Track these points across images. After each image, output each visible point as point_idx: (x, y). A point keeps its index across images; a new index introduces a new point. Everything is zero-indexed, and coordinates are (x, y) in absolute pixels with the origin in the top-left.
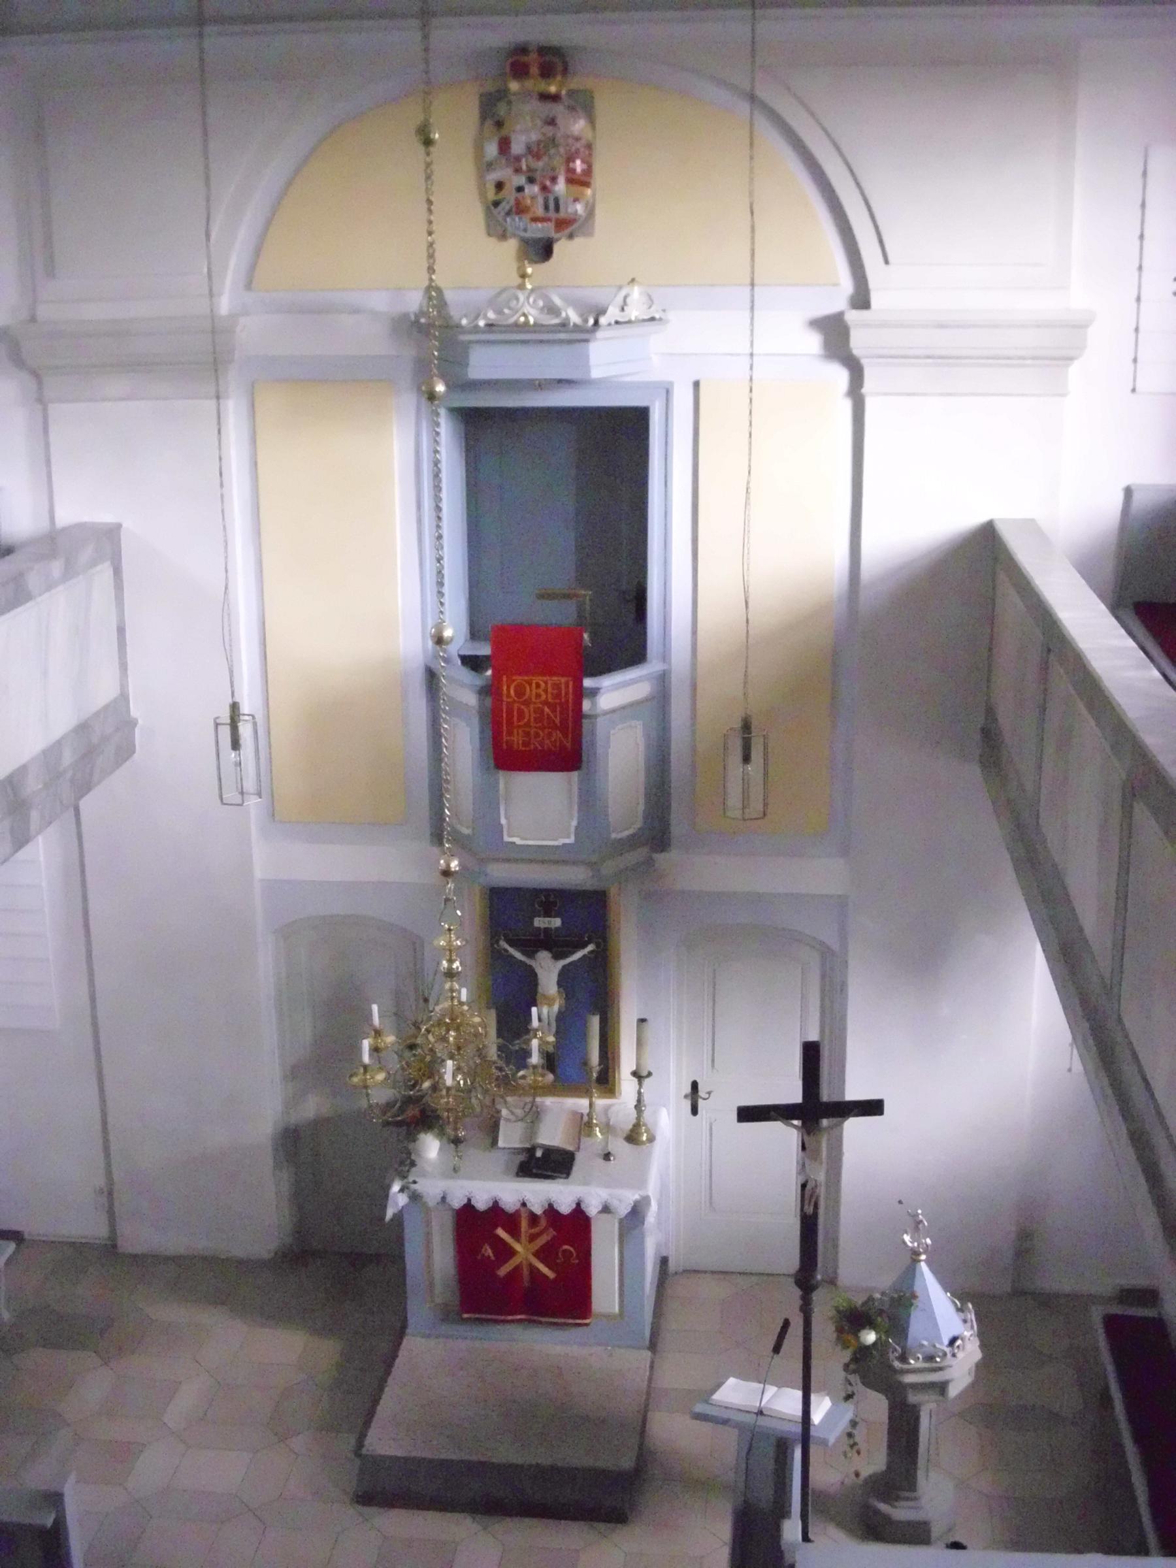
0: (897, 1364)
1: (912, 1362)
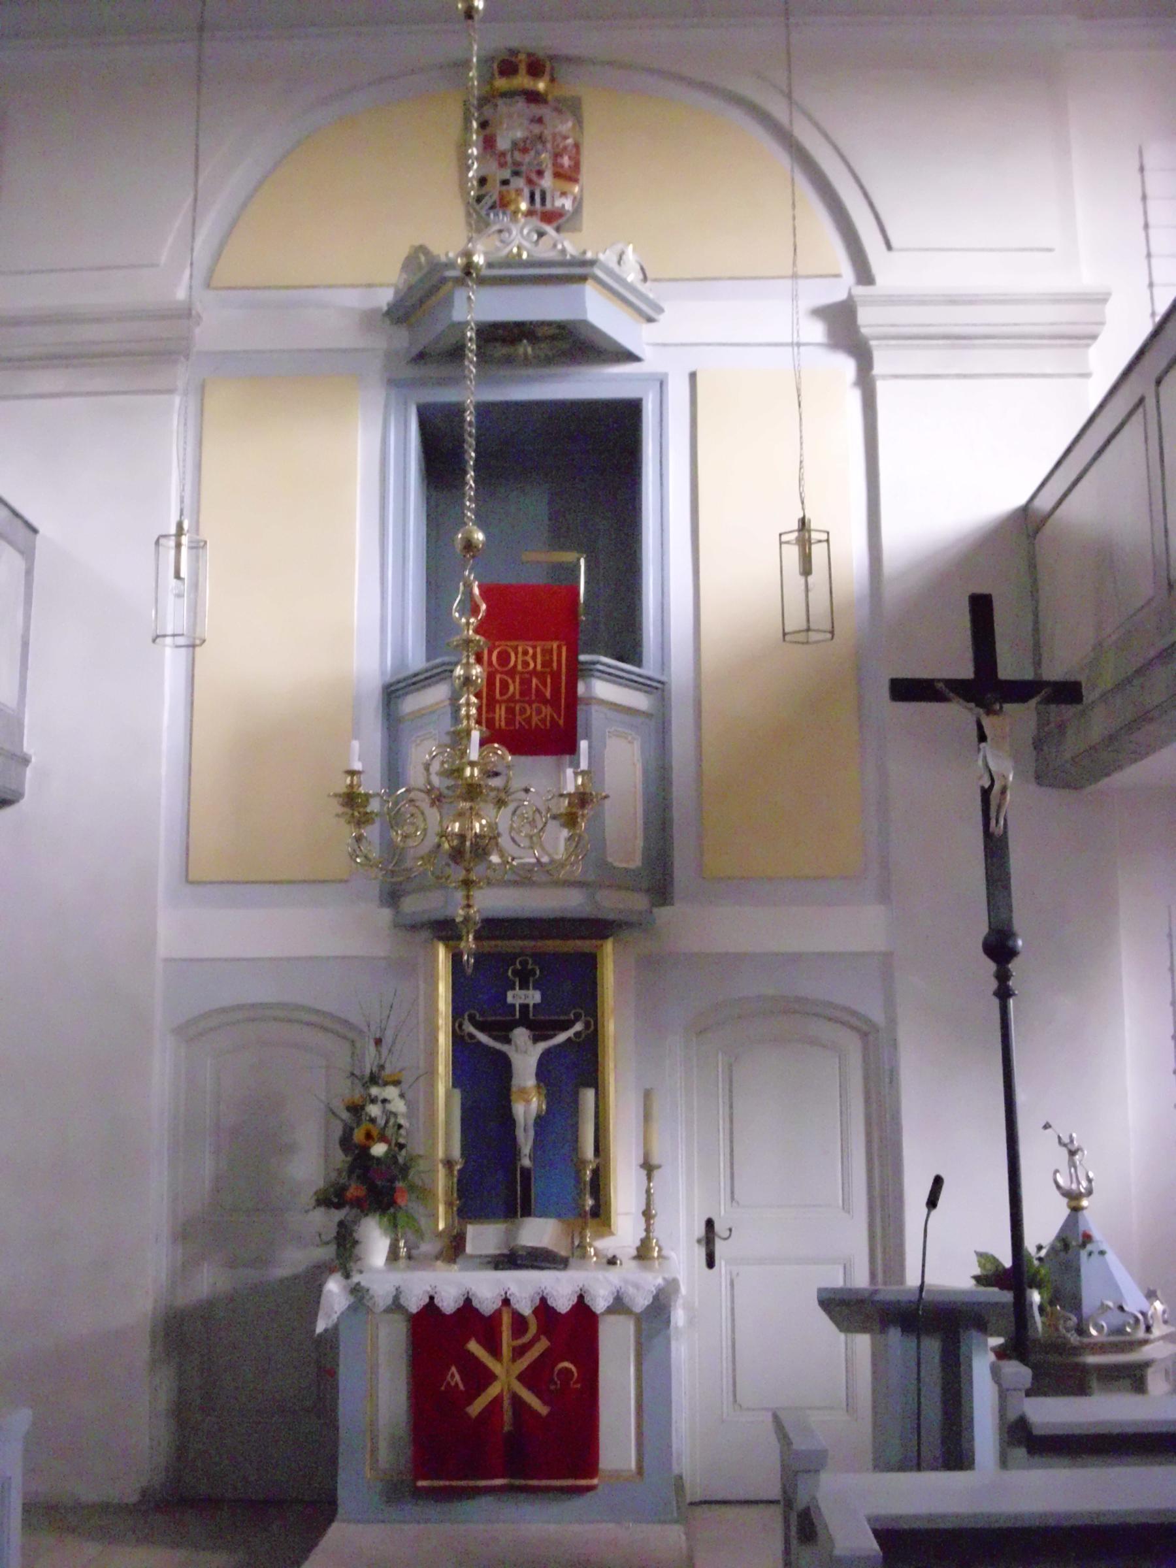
0: (1074, 1338)
1: (1093, 1332)
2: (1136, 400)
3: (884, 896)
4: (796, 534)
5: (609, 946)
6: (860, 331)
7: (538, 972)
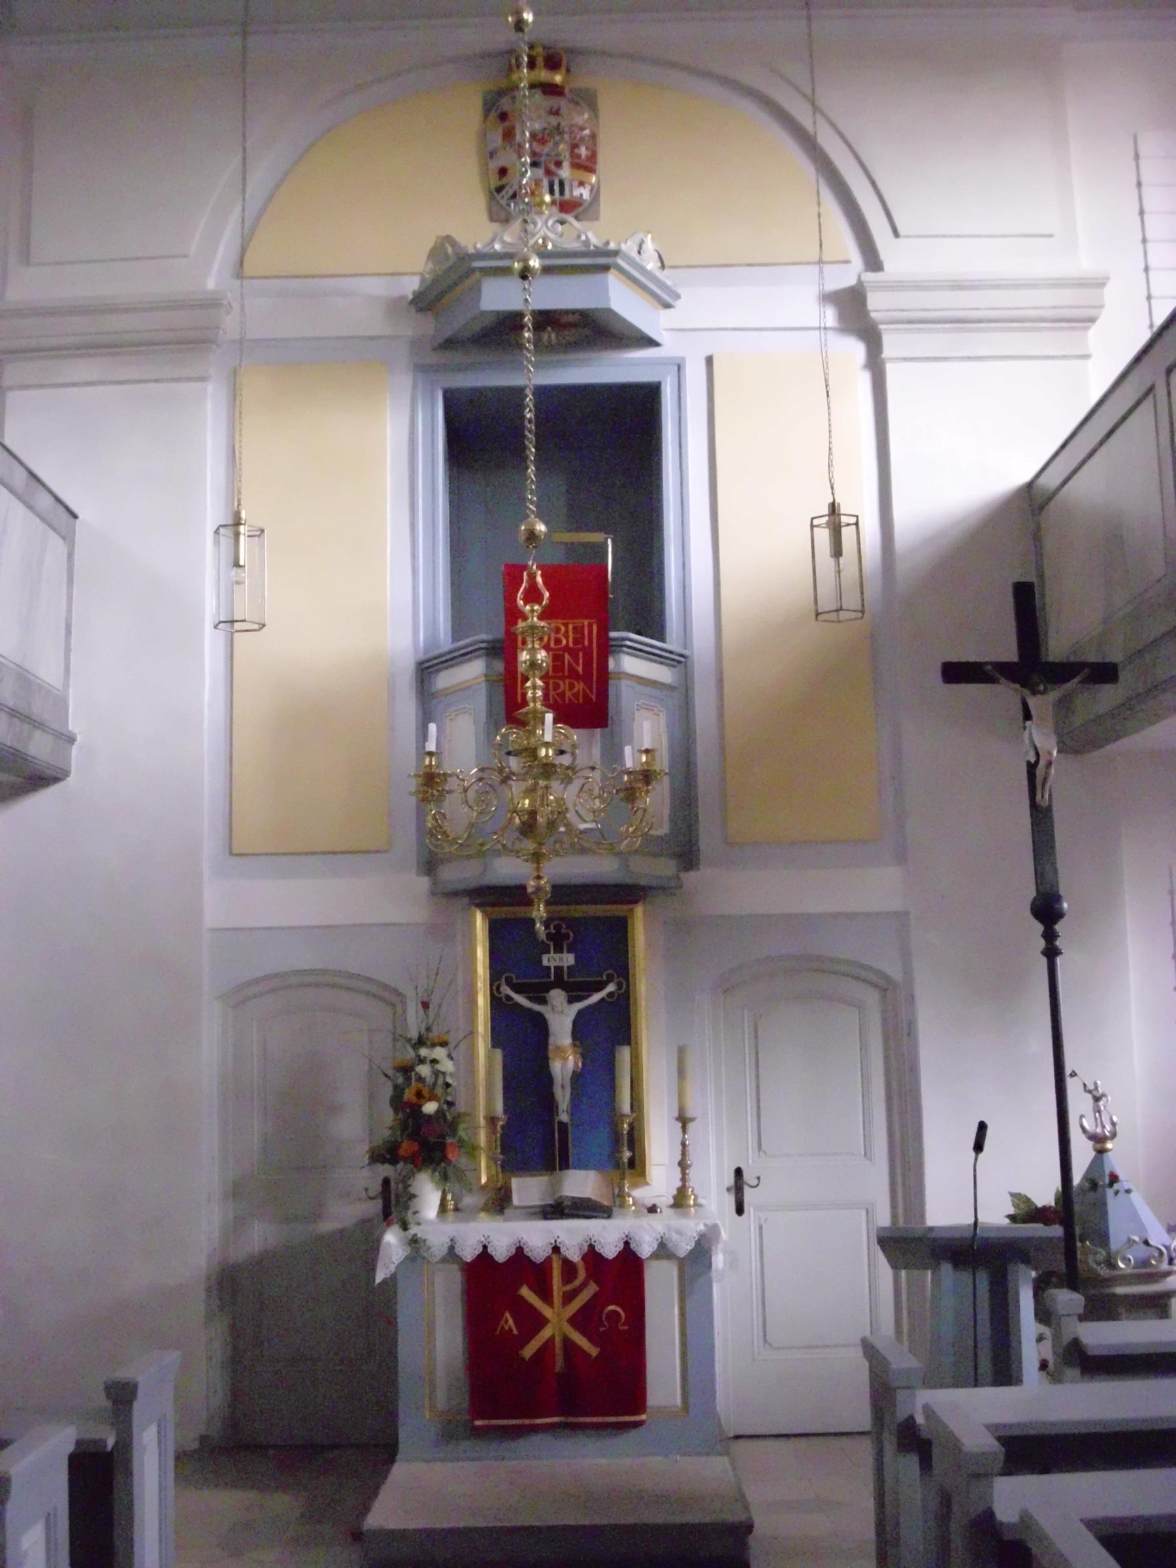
0: (1104, 1272)
1: (1121, 1265)
2: (1143, 390)
3: (901, 856)
4: (827, 518)
5: (639, 910)
6: (869, 316)
7: (571, 935)
